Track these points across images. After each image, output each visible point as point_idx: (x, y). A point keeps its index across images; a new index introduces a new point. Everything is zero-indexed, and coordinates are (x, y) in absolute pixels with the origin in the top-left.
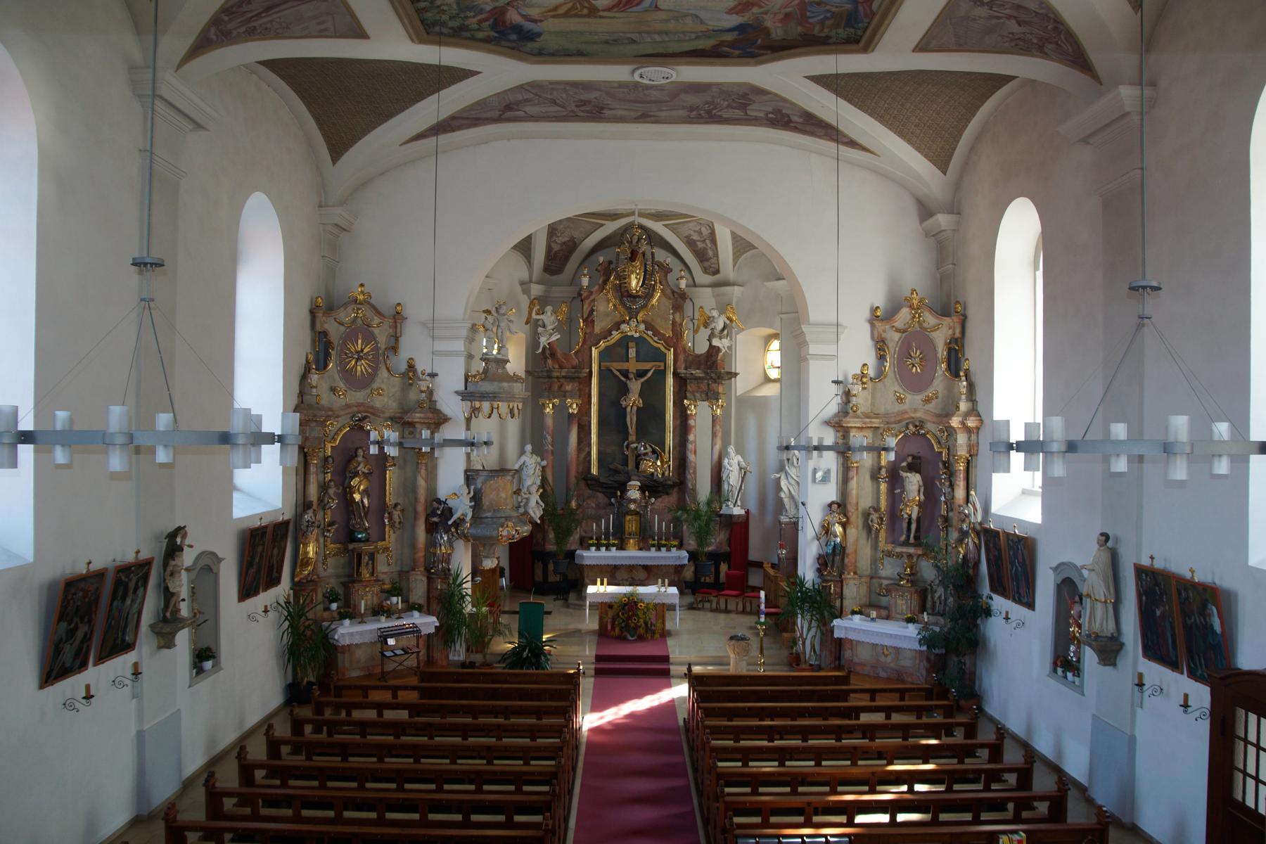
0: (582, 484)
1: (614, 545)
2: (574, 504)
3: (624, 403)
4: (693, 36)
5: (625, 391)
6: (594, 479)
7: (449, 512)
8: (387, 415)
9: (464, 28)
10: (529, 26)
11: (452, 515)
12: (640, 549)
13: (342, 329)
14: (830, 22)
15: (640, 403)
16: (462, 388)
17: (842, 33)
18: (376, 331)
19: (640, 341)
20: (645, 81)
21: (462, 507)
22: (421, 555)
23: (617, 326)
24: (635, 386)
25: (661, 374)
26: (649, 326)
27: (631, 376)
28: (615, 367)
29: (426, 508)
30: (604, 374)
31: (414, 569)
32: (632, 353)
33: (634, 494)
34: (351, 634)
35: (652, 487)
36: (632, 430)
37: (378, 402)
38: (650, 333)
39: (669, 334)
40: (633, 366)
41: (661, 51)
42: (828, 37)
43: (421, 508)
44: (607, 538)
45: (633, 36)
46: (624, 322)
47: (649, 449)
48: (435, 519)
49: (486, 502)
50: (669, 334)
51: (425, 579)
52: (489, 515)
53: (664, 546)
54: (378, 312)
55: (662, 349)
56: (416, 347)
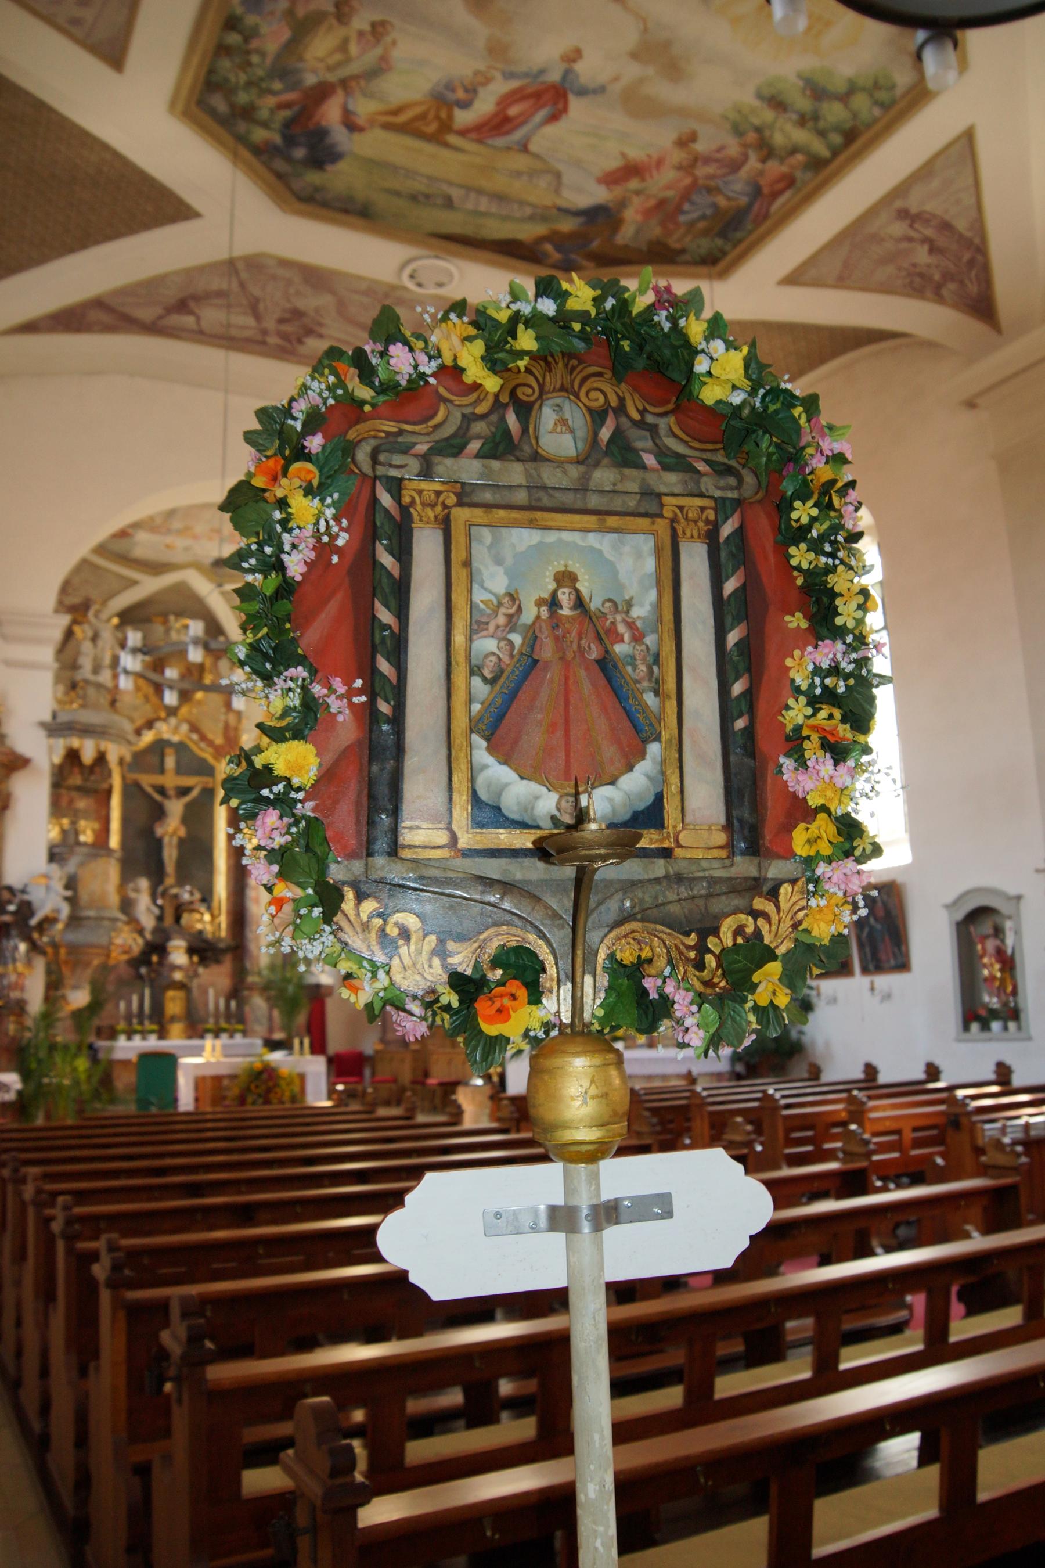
1: (152, 1032)
3: (159, 831)
4: (528, 211)
5: (159, 813)
7: (26, 909)
9: (247, 113)
10: (339, 135)
11: (32, 913)
14: (701, 225)
15: (182, 832)
16: (47, 717)
17: (704, 245)
19: (181, 748)
20: (410, 285)
21: (49, 900)
23: (150, 725)
24: (175, 808)
25: (208, 793)
26: (194, 728)
27: (171, 793)
28: (147, 781)
30: (132, 790)
32: (170, 762)
33: (178, 956)
35: (203, 950)
36: (170, 867)
38: (195, 737)
39: (219, 741)
40: (171, 780)
41: (469, 231)
42: (683, 251)
44: (141, 1023)
45: (455, 193)
46: (159, 719)
47: (197, 896)
49: (84, 897)
50: (219, 741)
52: (91, 913)
53: (224, 1030)
55: (211, 760)
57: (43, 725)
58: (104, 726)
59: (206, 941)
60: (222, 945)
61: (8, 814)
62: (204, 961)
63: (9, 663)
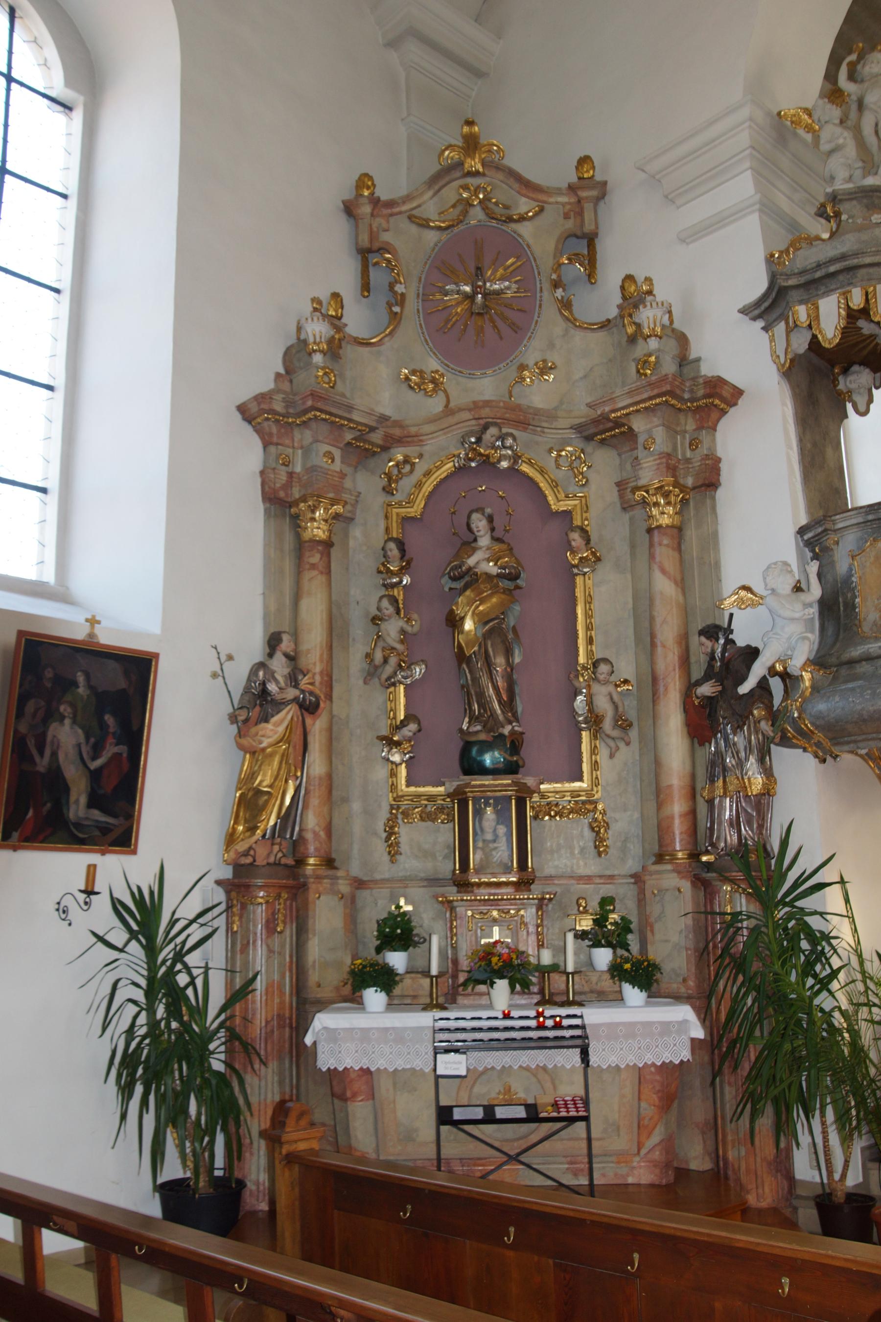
8: (567, 423)
13: (431, 237)
18: (525, 230)
22: (677, 808)
29: (685, 661)
31: (660, 858)
34: (365, 1034)
37: (538, 394)
43: (668, 660)
48: (707, 689)
51: (686, 886)
54: (527, 186)
56: (638, 242)
57: (744, 311)
58: (843, 257)
61: (720, 493)
63: (688, 237)
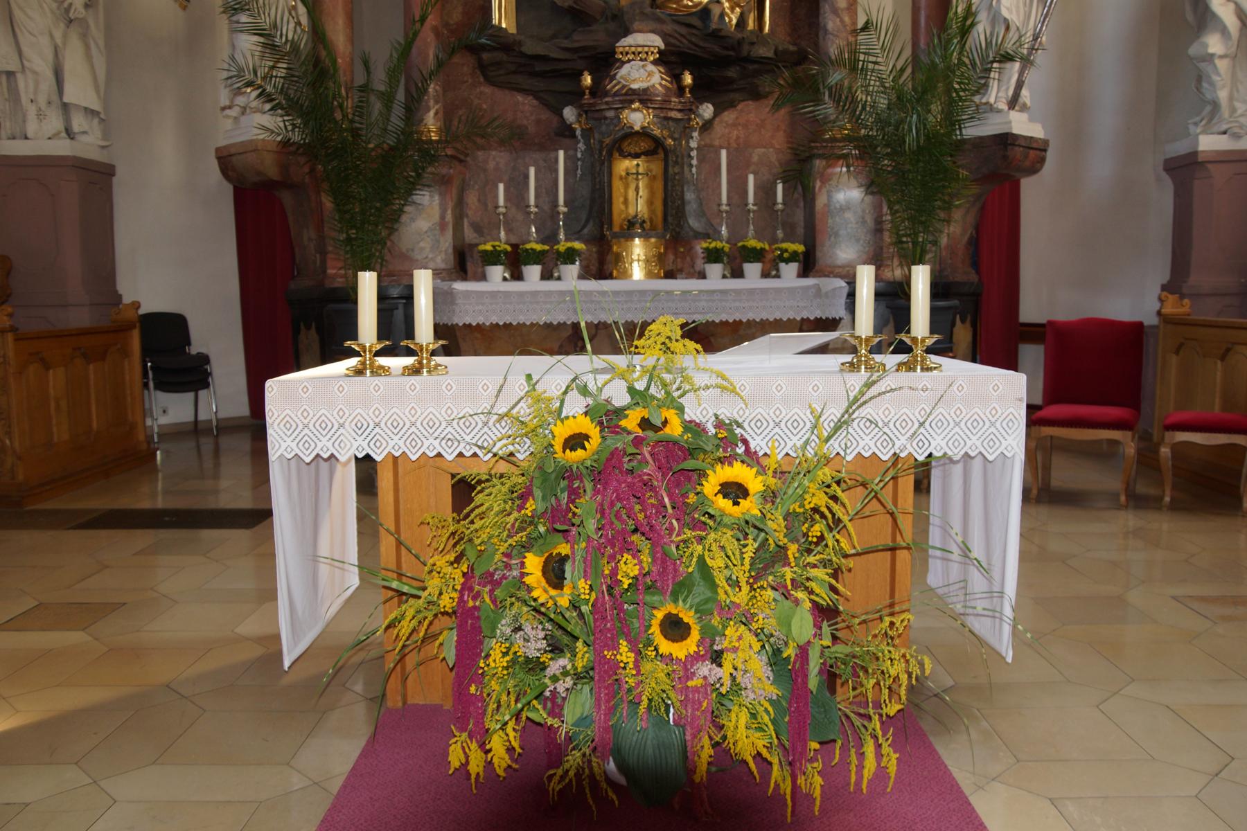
0: (464, 64)
1: (569, 257)
2: (431, 124)
6: (503, 43)
12: (670, 275)
33: (641, 73)
53: (756, 255)
59: (717, 36)
60: (765, 52)
62: (705, 89)
